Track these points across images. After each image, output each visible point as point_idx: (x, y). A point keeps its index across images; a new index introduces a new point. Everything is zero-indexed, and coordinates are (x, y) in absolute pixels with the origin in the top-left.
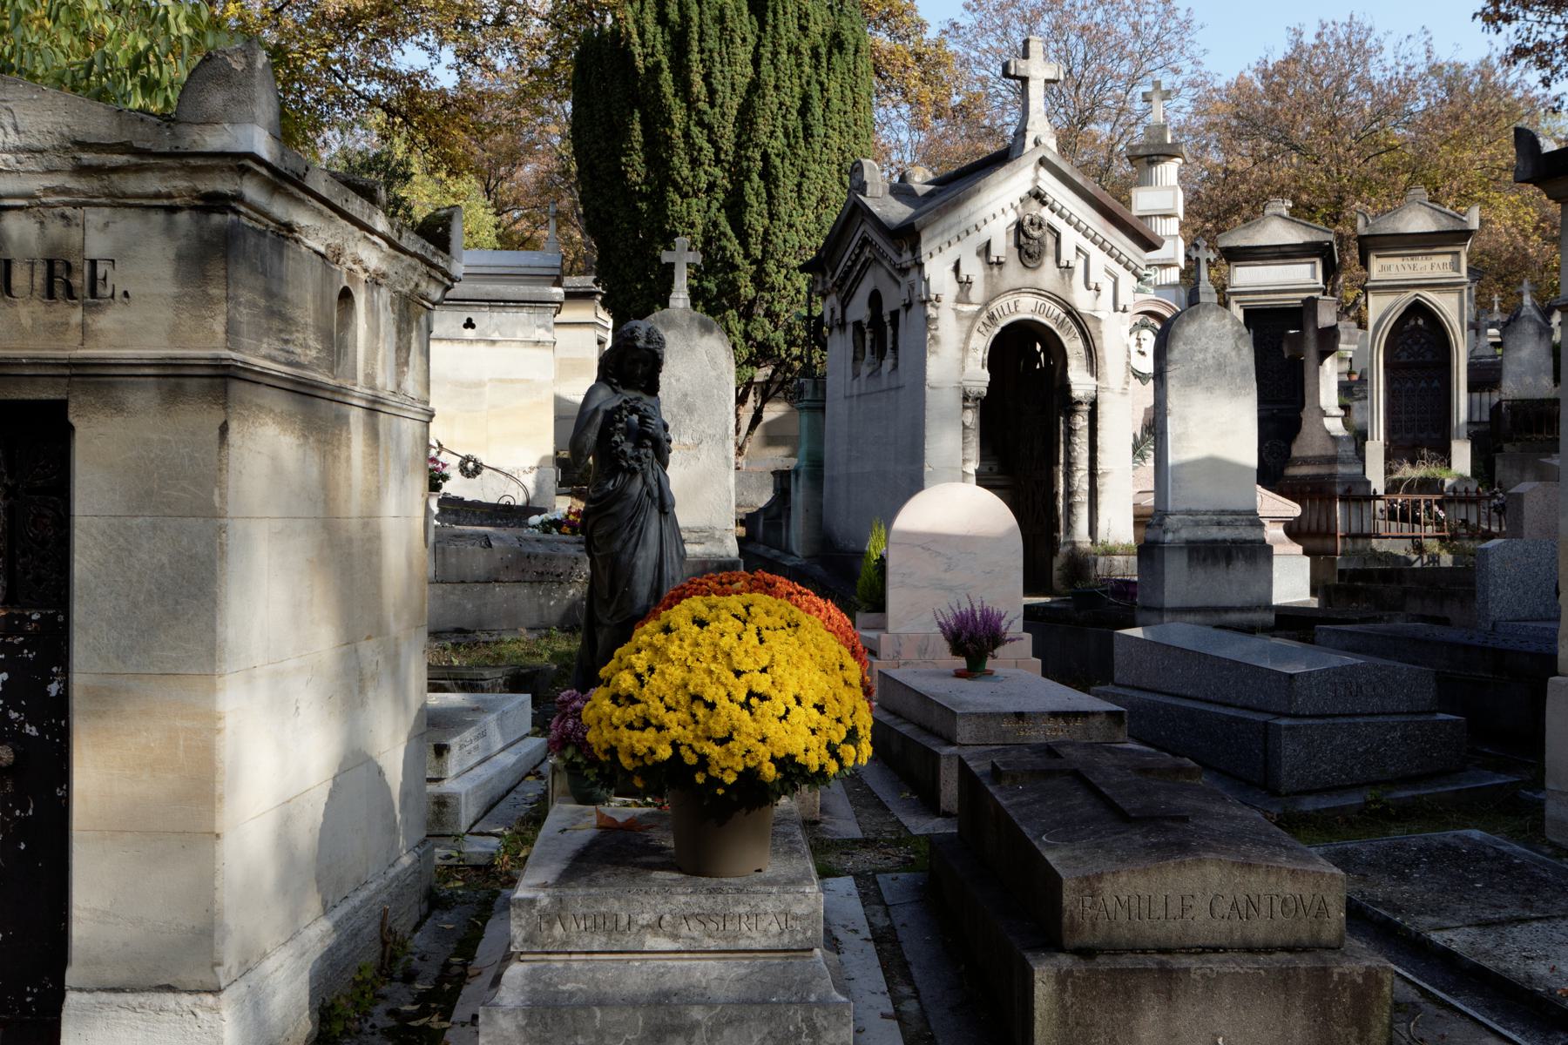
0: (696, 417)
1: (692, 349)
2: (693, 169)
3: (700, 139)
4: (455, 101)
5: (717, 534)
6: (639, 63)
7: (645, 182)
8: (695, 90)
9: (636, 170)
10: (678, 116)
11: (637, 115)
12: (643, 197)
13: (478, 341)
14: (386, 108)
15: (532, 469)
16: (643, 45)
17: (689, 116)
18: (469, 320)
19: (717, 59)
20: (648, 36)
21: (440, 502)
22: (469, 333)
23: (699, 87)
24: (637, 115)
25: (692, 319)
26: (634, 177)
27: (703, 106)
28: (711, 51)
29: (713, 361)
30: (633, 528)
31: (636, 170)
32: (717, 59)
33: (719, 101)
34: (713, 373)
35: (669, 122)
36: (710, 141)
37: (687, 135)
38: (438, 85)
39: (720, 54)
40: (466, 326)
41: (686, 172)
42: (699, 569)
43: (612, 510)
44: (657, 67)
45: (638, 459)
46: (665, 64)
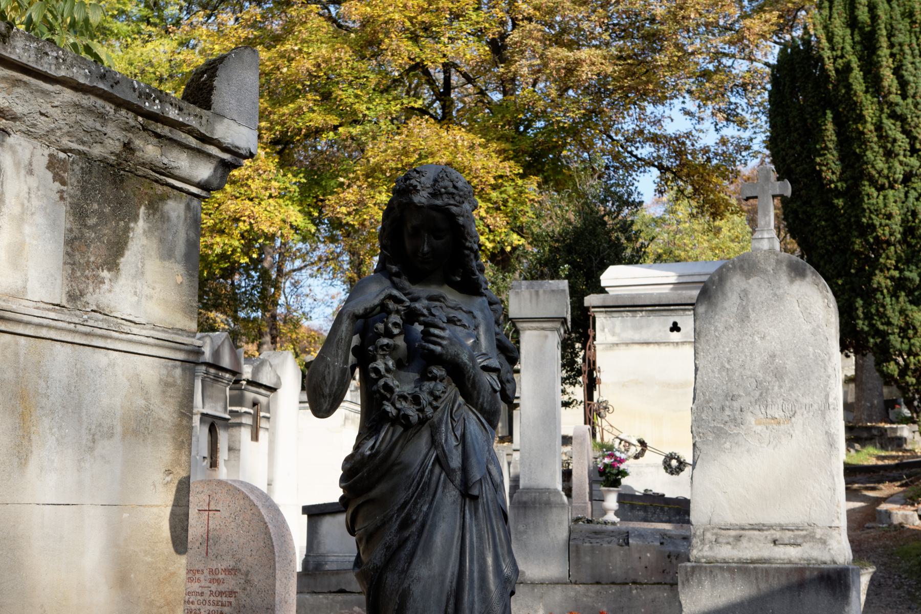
0: (787, 383)
1: (779, 298)
2: (887, 162)
3: (893, 129)
4: (716, 154)
5: (819, 534)
6: (829, 66)
7: (840, 179)
8: (885, 84)
9: (831, 167)
10: (870, 111)
11: (829, 115)
12: (838, 194)
13: (683, 343)
14: (660, 167)
16: (832, 49)
17: (882, 111)
18: (675, 324)
19: (908, 51)
20: (837, 39)
21: (622, 498)
22: (675, 336)
23: (889, 79)
24: (829, 115)
25: (779, 262)
26: (829, 175)
27: (895, 98)
28: (901, 45)
29: (807, 313)
30: (405, 524)
31: (831, 167)
32: (908, 51)
33: (911, 92)
34: (807, 327)
35: (861, 118)
36: (904, 132)
37: (879, 128)
39: (910, 45)
40: (672, 330)
41: (880, 165)
42: (795, 578)
43: (374, 493)
44: (848, 68)
45: (416, 400)
46: (855, 64)
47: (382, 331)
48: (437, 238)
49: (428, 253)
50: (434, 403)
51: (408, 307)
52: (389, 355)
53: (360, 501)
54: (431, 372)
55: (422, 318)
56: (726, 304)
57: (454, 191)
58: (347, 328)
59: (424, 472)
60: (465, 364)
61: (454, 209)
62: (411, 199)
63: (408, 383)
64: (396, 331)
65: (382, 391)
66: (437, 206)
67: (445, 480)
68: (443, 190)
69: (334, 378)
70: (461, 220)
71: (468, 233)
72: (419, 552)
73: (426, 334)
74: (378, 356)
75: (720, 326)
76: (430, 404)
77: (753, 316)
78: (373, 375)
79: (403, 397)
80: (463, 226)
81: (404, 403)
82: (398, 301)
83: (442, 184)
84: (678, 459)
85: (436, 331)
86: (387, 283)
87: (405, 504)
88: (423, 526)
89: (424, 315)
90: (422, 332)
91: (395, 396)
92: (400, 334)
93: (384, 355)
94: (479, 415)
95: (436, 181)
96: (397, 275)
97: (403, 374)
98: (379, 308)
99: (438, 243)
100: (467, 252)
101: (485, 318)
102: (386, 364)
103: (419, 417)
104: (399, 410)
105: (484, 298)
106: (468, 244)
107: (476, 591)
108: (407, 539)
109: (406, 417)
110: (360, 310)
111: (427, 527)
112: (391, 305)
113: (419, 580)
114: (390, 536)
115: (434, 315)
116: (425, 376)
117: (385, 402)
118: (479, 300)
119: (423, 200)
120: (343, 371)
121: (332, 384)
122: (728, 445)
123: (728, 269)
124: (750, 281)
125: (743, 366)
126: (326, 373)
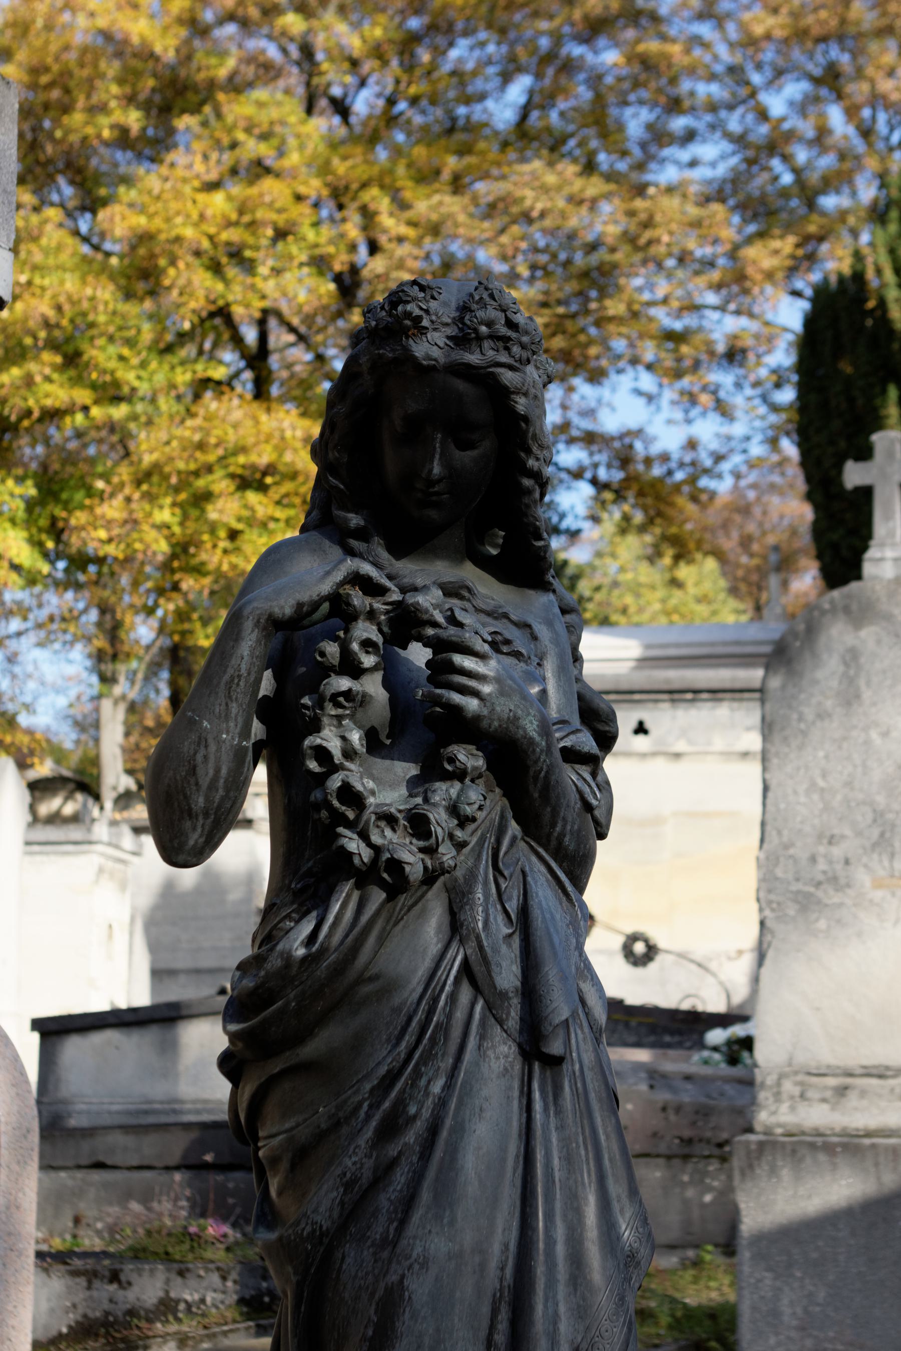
4: (681, 465)
13: (654, 754)
14: (594, 482)
15: (740, 953)
30: (391, 1127)
38: (656, 449)
43: (310, 1050)
45: (419, 825)
47: (336, 661)
48: (465, 446)
49: (439, 481)
50: (459, 833)
51: (398, 604)
52: (352, 717)
53: (276, 1066)
54: (452, 760)
55: (430, 632)
56: (820, 674)
57: (510, 333)
58: (253, 650)
59: (435, 1000)
60: (531, 741)
61: (508, 377)
62: (407, 350)
63: (393, 786)
64: (368, 661)
65: (336, 803)
66: (469, 366)
67: (483, 1023)
68: (484, 329)
69: (218, 771)
70: (521, 404)
71: (535, 437)
72: (425, 1196)
73: (441, 670)
74: (325, 720)
75: (809, 713)
76: (451, 836)
77: (867, 695)
78: (313, 765)
79: (390, 820)
80: (526, 419)
81: (388, 832)
82: (372, 588)
83: (480, 314)
84: (646, 941)
85: (468, 663)
86: (336, 552)
87: (392, 1077)
88: (433, 1130)
89: (435, 625)
90: (429, 664)
91: (369, 815)
92: (374, 669)
93: (339, 718)
94: (554, 865)
95: (464, 309)
96: (362, 534)
97: (380, 764)
98: (326, 606)
99: (465, 458)
100: (527, 482)
101: (556, 642)
102: (344, 738)
103: (426, 868)
104: (377, 850)
105: (551, 596)
106: (531, 463)
107: (562, 1290)
108: (393, 1163)
109: (396, 866)
110: (285, 607)
111: (444, 1134)
112: (358, 599)
113: (424, 1264)
114: (356, 1157)
115: (460, 625)
116: (433, 769)
117: (341, 830)
118: (544, 599)
119: (436, 353)
120: (239, 756)
121: (212, 786)
122: (822, 924)
123: (823, 613)
124: (863, 633)
125: (849, 784)
126: (199, 758)
